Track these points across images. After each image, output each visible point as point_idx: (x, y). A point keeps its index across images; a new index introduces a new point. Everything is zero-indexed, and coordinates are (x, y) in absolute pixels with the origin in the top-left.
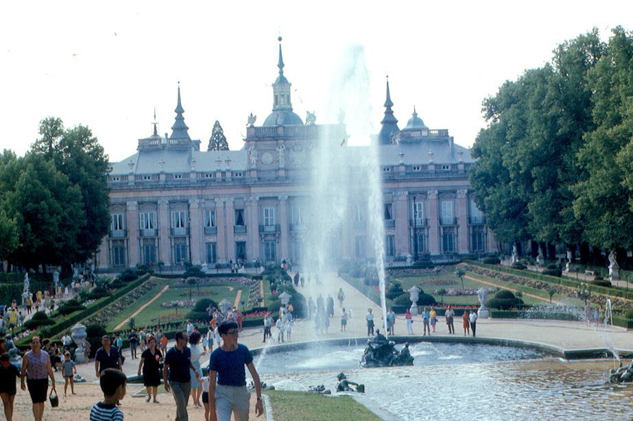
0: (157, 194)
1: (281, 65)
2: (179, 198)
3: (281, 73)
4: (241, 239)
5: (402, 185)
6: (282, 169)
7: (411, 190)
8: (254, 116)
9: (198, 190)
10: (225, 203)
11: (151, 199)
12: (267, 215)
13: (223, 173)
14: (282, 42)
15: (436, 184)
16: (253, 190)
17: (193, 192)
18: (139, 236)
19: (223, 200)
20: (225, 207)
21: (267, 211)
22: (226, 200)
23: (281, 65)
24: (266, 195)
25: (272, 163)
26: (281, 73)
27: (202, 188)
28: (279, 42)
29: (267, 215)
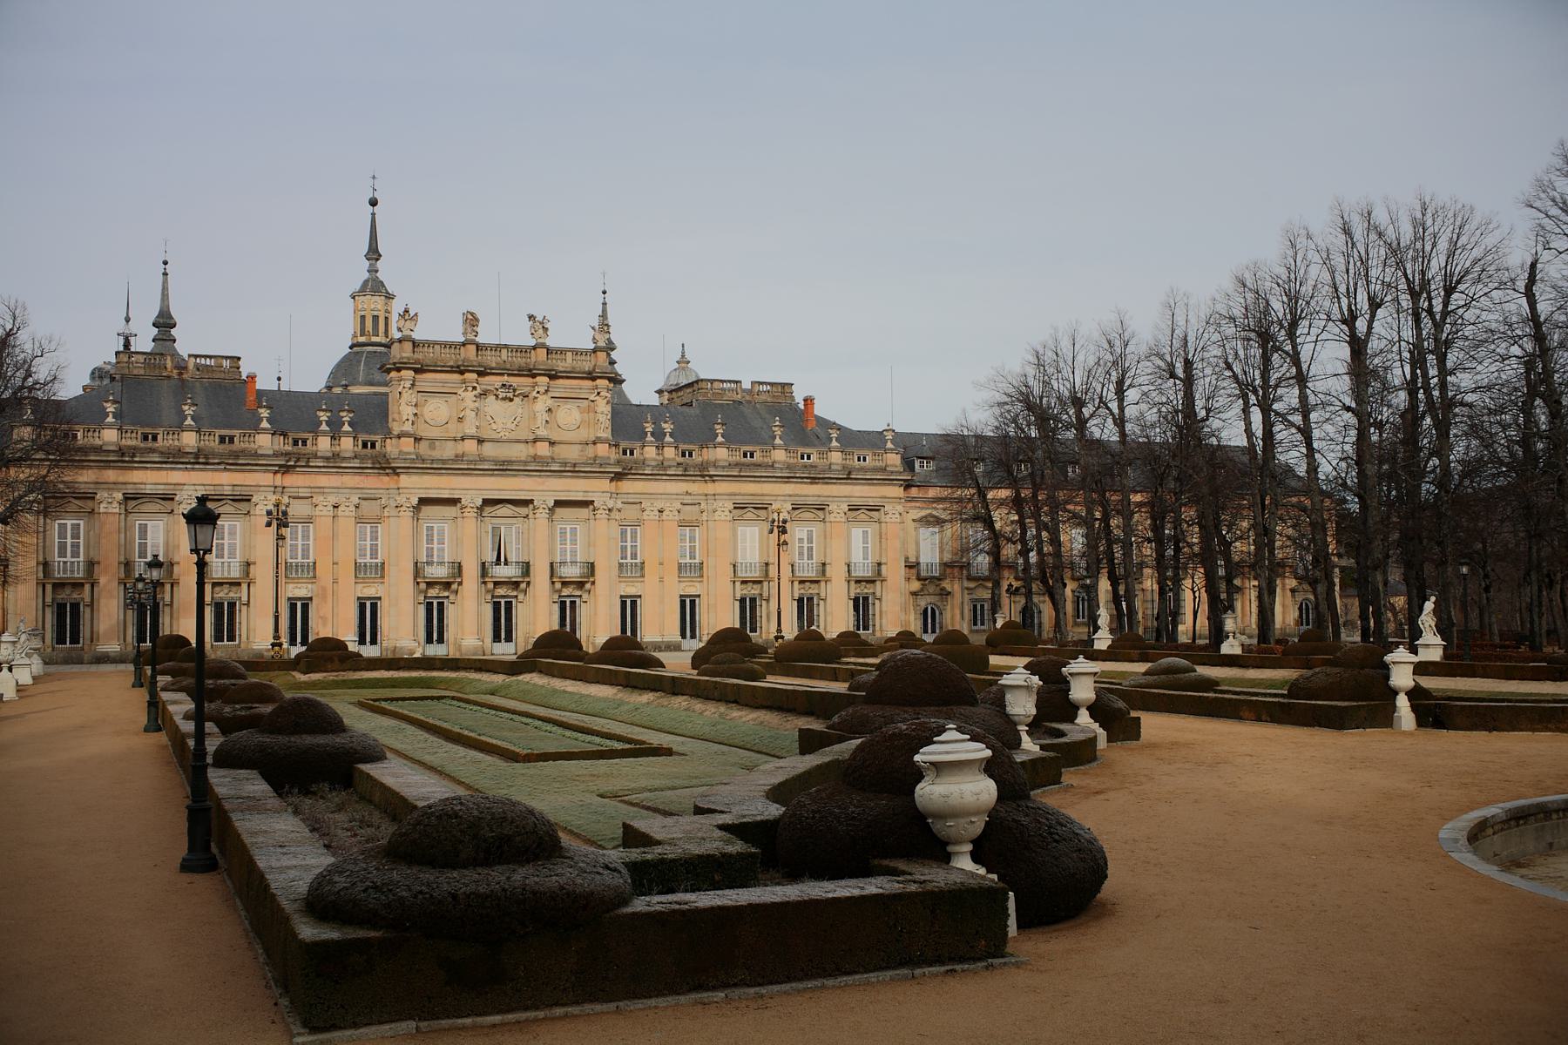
0: (176, 476)
1: (374, 253)
2: (227, 490)
3: (373, 270)
4: (370, 591)
5: (722, 487)
6: (472, 437)
7: (740, 499)
9: (276, 472)
11: (161, 489)
12: (430, 540)
15: (789, 488)
16: (405, 480)
17: (265, 478)
18: (122, 575)
19: (332, 499)
21: (430, 529)
23: (374, 253)
24: (433, 494)
26: (373, 270)
27: (286, 469)
29: (430, 540)
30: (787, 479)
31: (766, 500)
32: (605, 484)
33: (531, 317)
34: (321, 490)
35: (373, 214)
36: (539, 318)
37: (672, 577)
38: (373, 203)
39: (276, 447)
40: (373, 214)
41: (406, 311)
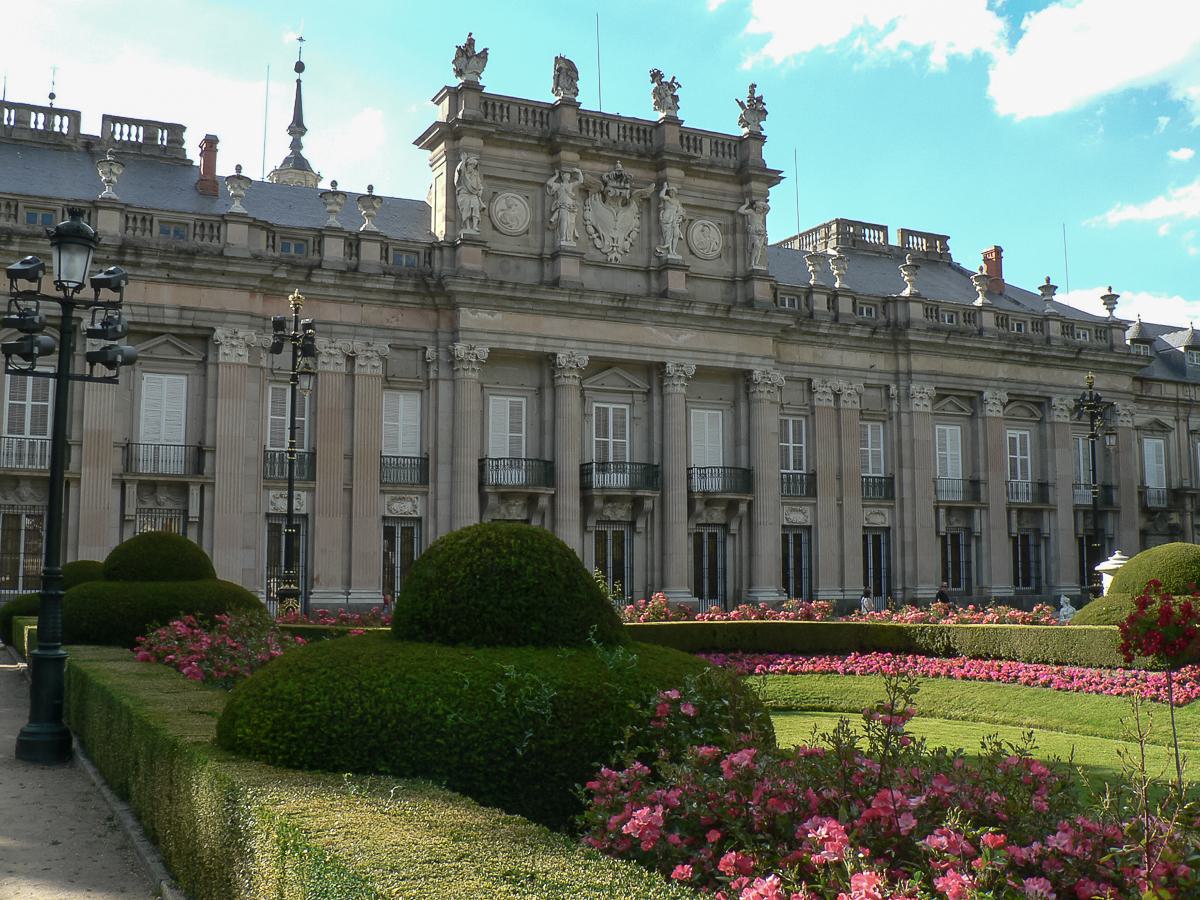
1: (297, 128)
2: (170, 317)
3: (296, 146)
7: (943, 382)
8: (478, 50)
10: (351, 359)
13: (354, 242)
14: (303, 76)
15: (1002, 370)
16: (468, 318)
17: (237, 300)
20: (351, 376)
22: (358, 345)
23: (297, 128)
24: (512, 343)
25: (527, 232)
26: (296, 146)
28: (296, 76)
30: (1001, 357)
31: (977, 385)
32: (767, 345)
33: (656, 75)
34: (330, 328)
35: (299, 82)
36: (667, 79)
37: (853, 501)
38: (300, 67)
39: (255, 250)
40: (299, 82)
41: (471, 42)
